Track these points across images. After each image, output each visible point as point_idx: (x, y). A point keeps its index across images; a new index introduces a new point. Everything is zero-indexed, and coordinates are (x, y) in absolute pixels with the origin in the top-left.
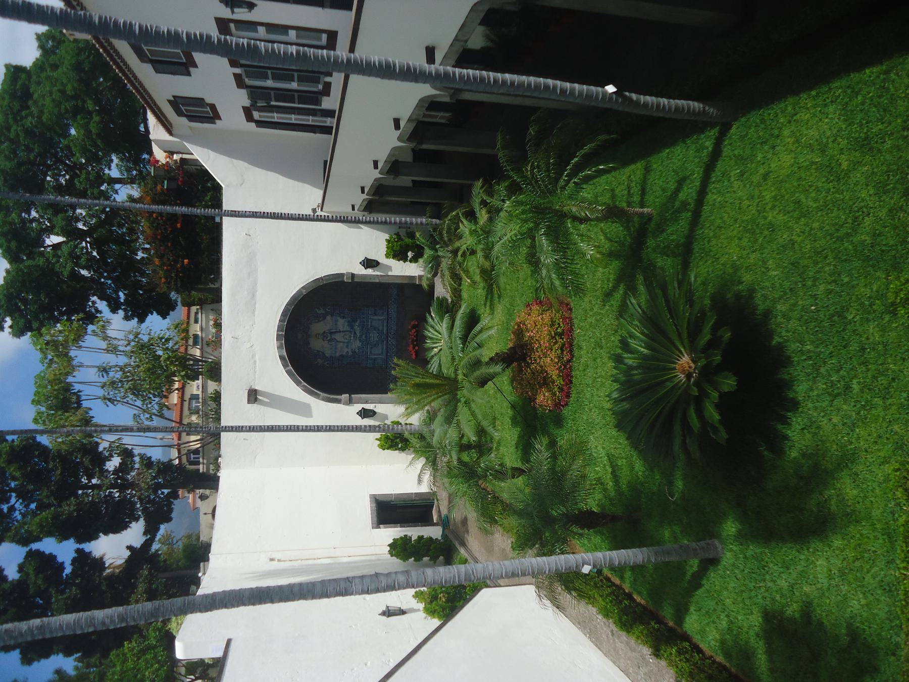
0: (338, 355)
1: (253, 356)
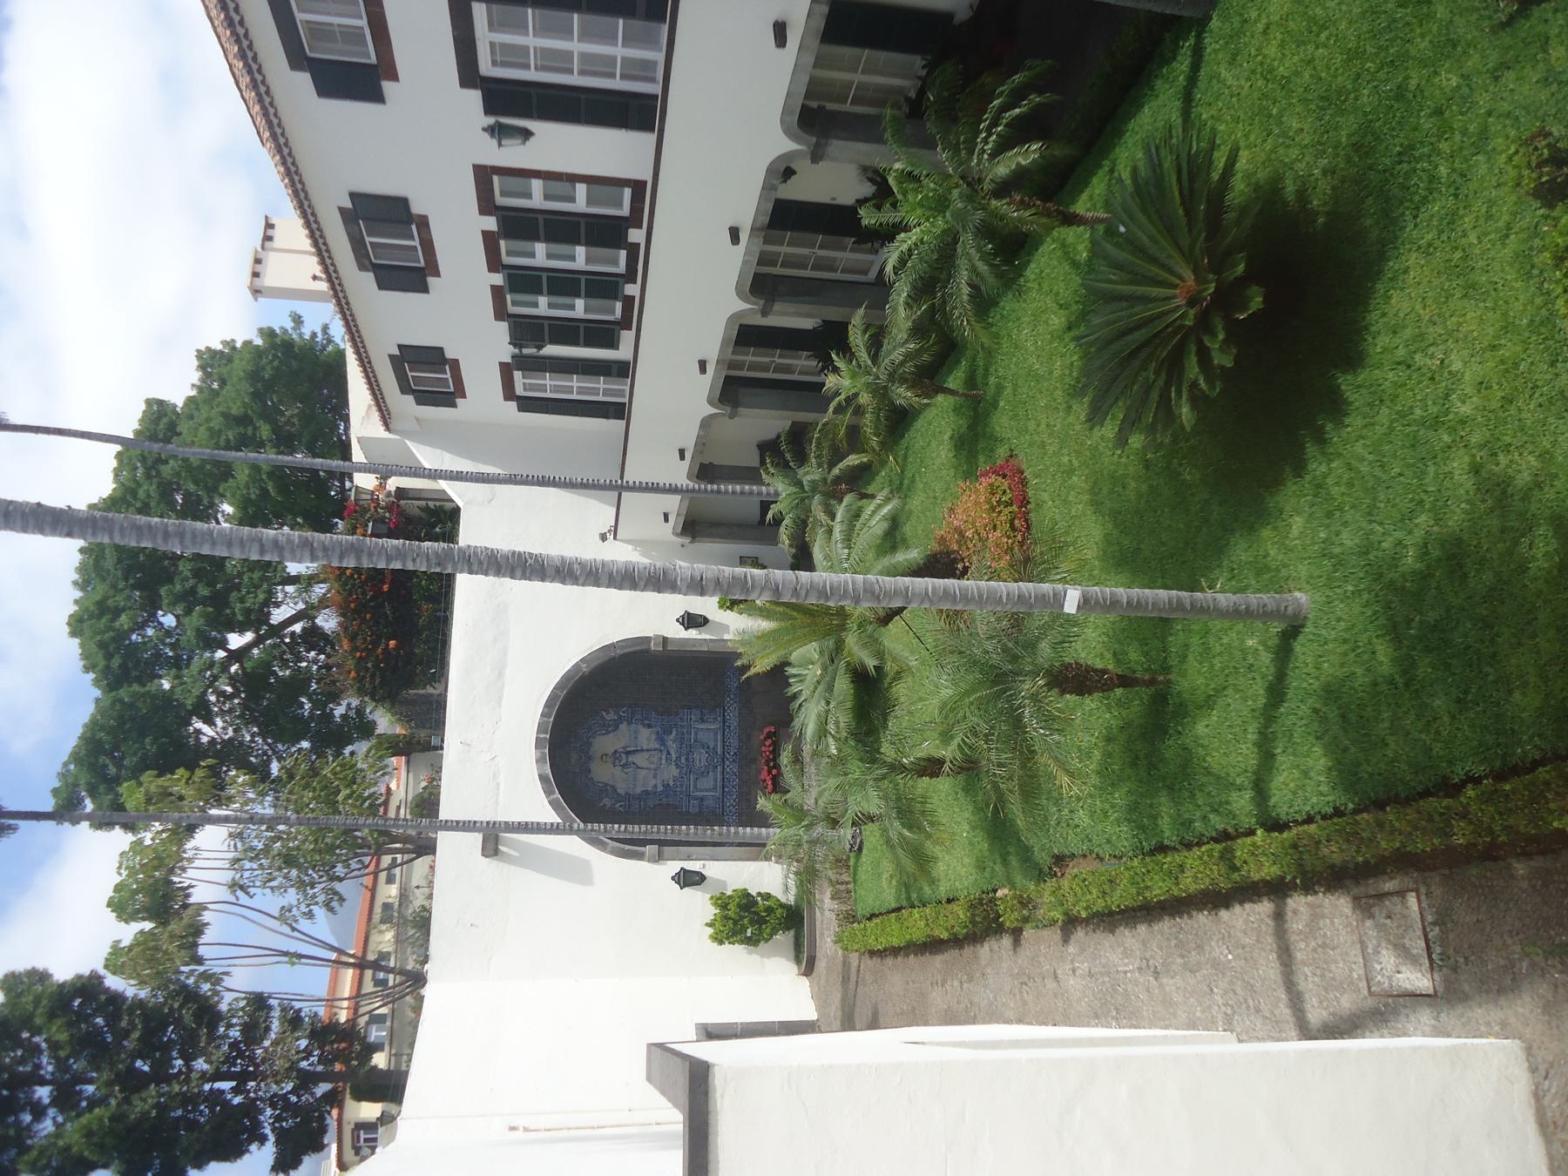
0: (638, 790)
1: (494, 776)
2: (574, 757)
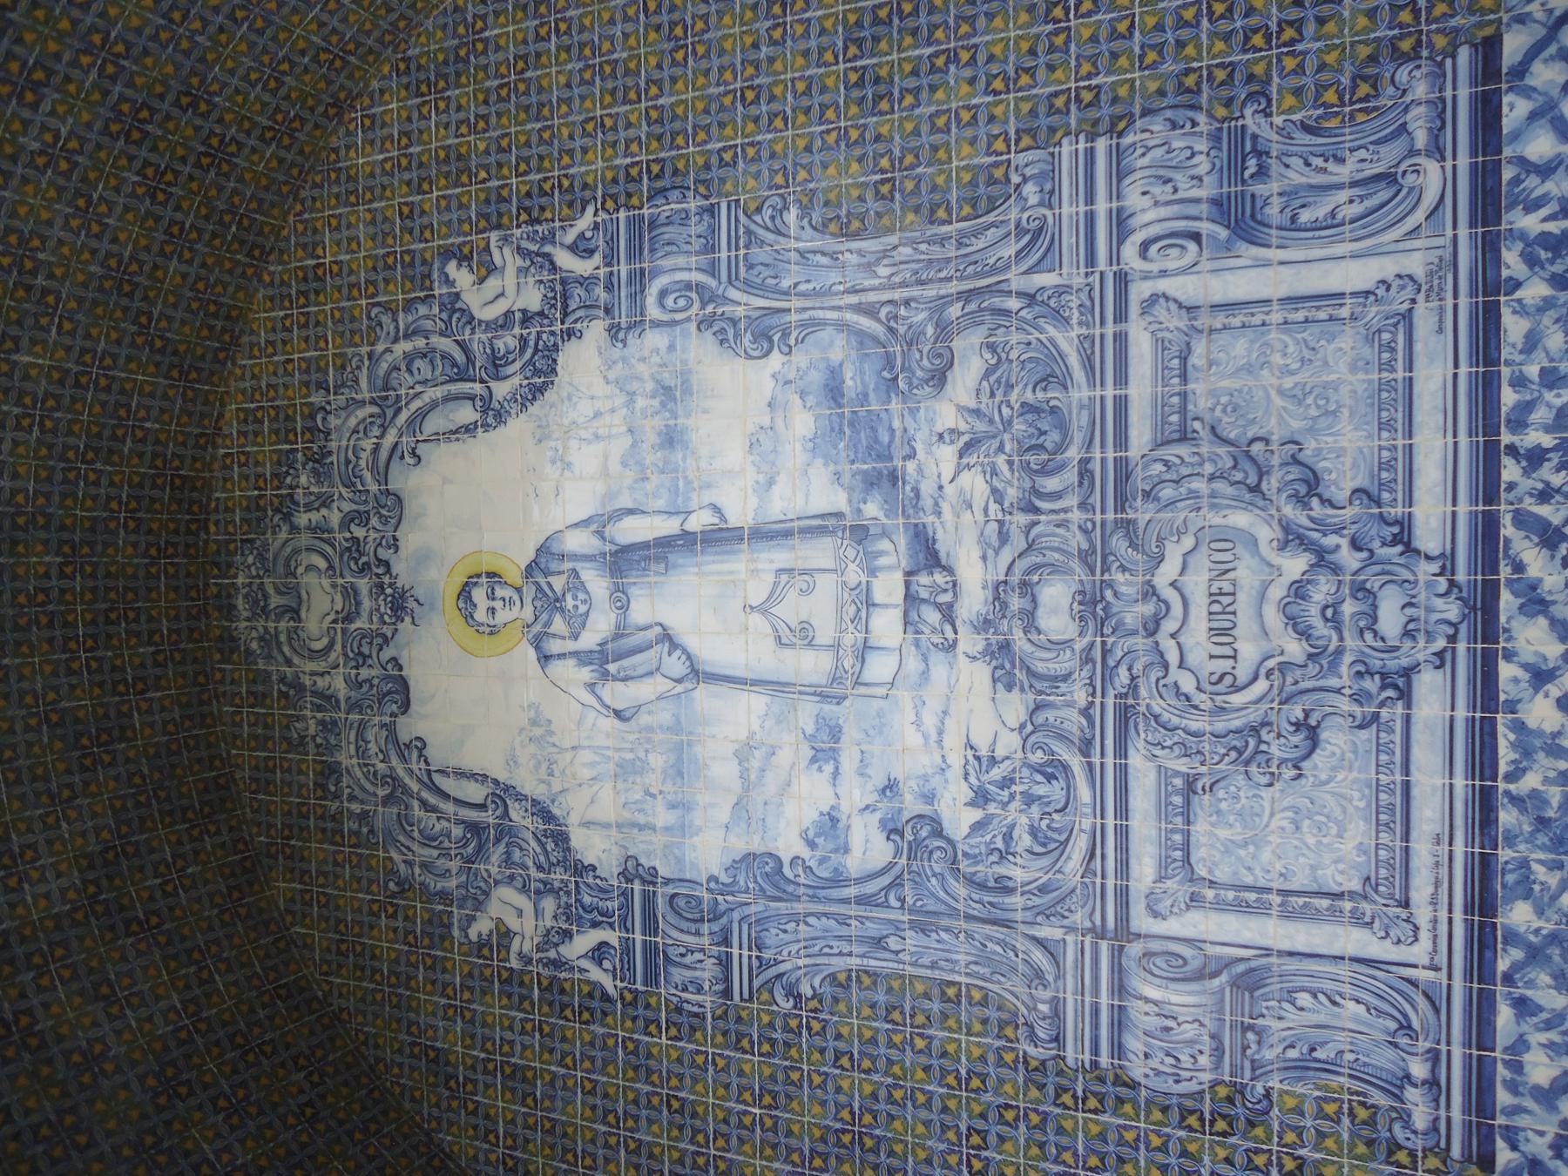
0: (708, 852)
2: (320, 601)
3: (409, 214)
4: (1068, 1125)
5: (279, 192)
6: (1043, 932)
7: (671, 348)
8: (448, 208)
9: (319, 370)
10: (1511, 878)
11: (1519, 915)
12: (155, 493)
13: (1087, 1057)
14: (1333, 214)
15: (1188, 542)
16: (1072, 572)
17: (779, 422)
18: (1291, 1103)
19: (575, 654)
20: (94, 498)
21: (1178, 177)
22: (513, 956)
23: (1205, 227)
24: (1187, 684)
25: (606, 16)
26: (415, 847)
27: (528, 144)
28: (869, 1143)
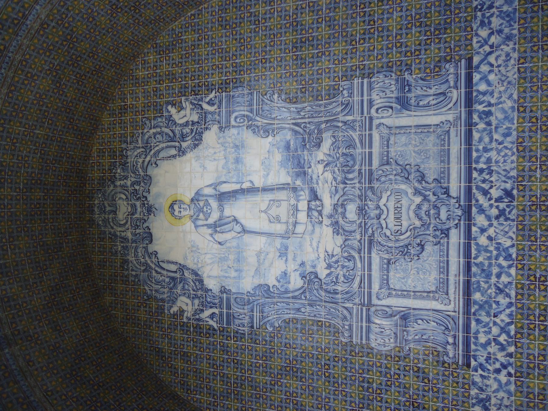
0: (247, 284)
2: (123, 209)
3: (156, 90)
4: (353, 361)
5: (114, 82)
6: (347, 305)
7: (238, 134)
8: (169, 89)
9: (125, 137)
10: (475, 286)
11: (477, 296)
12: (71, 174)
13: (359, 341)
14: (428, 103)
15: (389, 193)
16: (356, 201)
17: (271, 157)
18: (416, 351)
19: (206, 225)
20: (54, 175)
21: (387, 91)
22: (184, 318)
23: (394, 105)
24: (388, 233)
25: (220, 35)
26: (153, 285)
27: (195, 71)
28: (295, 370)
